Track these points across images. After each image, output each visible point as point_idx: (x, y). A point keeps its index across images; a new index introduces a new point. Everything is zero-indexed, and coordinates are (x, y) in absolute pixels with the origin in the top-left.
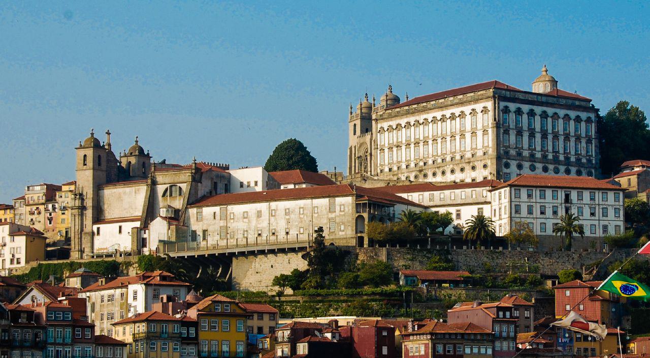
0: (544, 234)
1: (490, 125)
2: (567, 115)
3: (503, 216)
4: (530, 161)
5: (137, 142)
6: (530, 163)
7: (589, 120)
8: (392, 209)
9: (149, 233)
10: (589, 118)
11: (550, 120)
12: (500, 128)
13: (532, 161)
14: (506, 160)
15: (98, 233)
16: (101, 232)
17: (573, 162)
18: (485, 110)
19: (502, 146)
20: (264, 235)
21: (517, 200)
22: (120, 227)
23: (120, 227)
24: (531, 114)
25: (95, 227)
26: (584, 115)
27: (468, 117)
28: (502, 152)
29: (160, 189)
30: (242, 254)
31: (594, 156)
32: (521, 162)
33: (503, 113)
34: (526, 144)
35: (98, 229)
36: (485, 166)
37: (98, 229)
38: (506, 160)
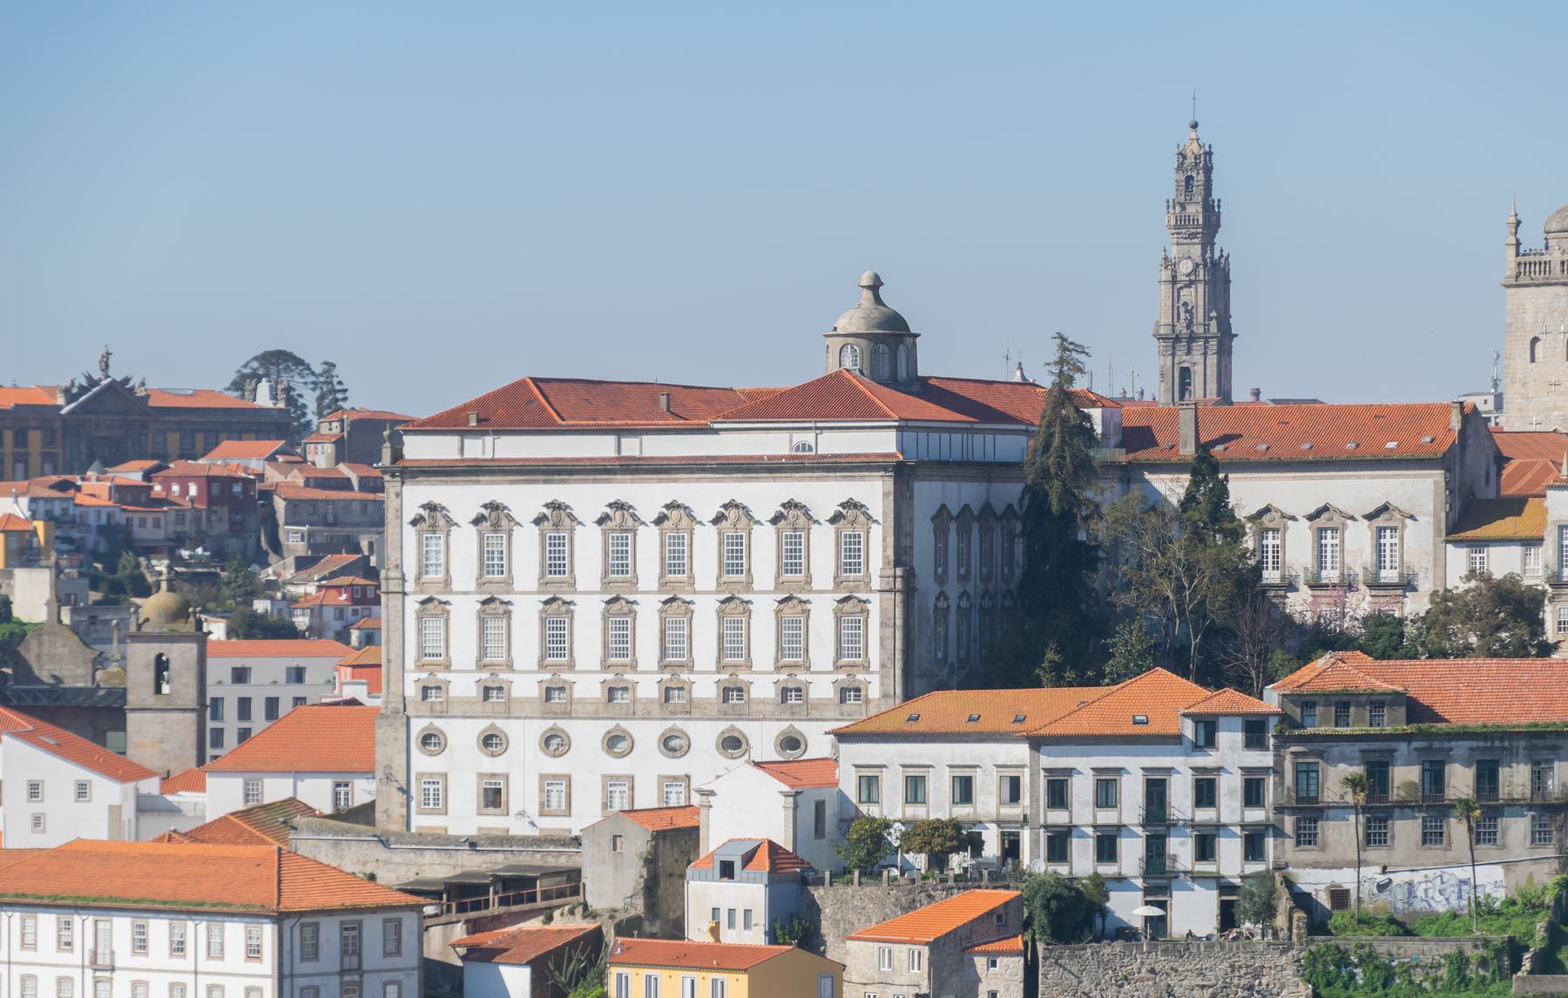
12: (404, 594)
13: (555, 715)
14: (424, 723)
17: (763, 702)
28: (412, 691)
31: (875, 665)
32: (499, 723)
38: (424, 723)
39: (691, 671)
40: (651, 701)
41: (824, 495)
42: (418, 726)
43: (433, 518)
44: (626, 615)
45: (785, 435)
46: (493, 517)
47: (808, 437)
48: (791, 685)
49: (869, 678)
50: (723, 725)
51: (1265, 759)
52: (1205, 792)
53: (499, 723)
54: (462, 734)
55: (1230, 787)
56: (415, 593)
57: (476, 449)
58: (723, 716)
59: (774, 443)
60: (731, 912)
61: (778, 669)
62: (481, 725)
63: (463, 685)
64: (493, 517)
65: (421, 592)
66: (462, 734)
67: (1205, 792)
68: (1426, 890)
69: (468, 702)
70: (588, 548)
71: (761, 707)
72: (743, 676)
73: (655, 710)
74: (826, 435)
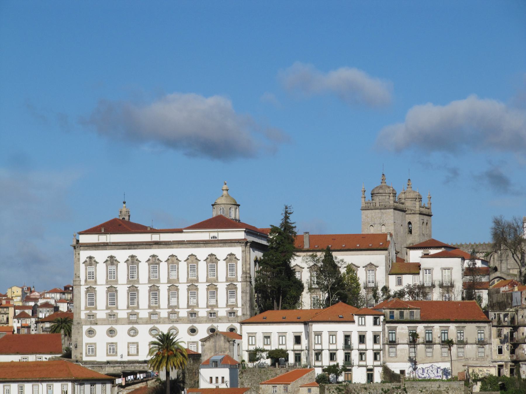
17: (203, 317)
19: (83, 307)
28: (83, 316)
31: (240, 305)
32: (114, 326)
33: (86, 266)
39: (179, 308)
40: (165, 318)
41: (222, 252)
42: (85, 328)
43: (91, 262)
44: (156, 291)
45: (208, 234)
46: (112, 261)
47: (215, 234)
48: (212, 312)
49: (237, 309)
50: (190, 325)
51: (379, 329)
52: (362, 339)
53: (114, 326)
54: (101, 330)
55: (369, 338)
56: (85, 285)
57: (103, 238)
58: (190, 322)
59: (204, 235)
60: (217, 378)
61: (207, 307)
62: (108, 327)
64: (112, 261)
65: (87, 285)
66: (101, 330)
67: (362, 339)
68: (427, 371)
69: (104, 320)
70: (144, 269)
71: (202, 319)
72: (196, 310)
73: (167, 320)
74: (220, 234)
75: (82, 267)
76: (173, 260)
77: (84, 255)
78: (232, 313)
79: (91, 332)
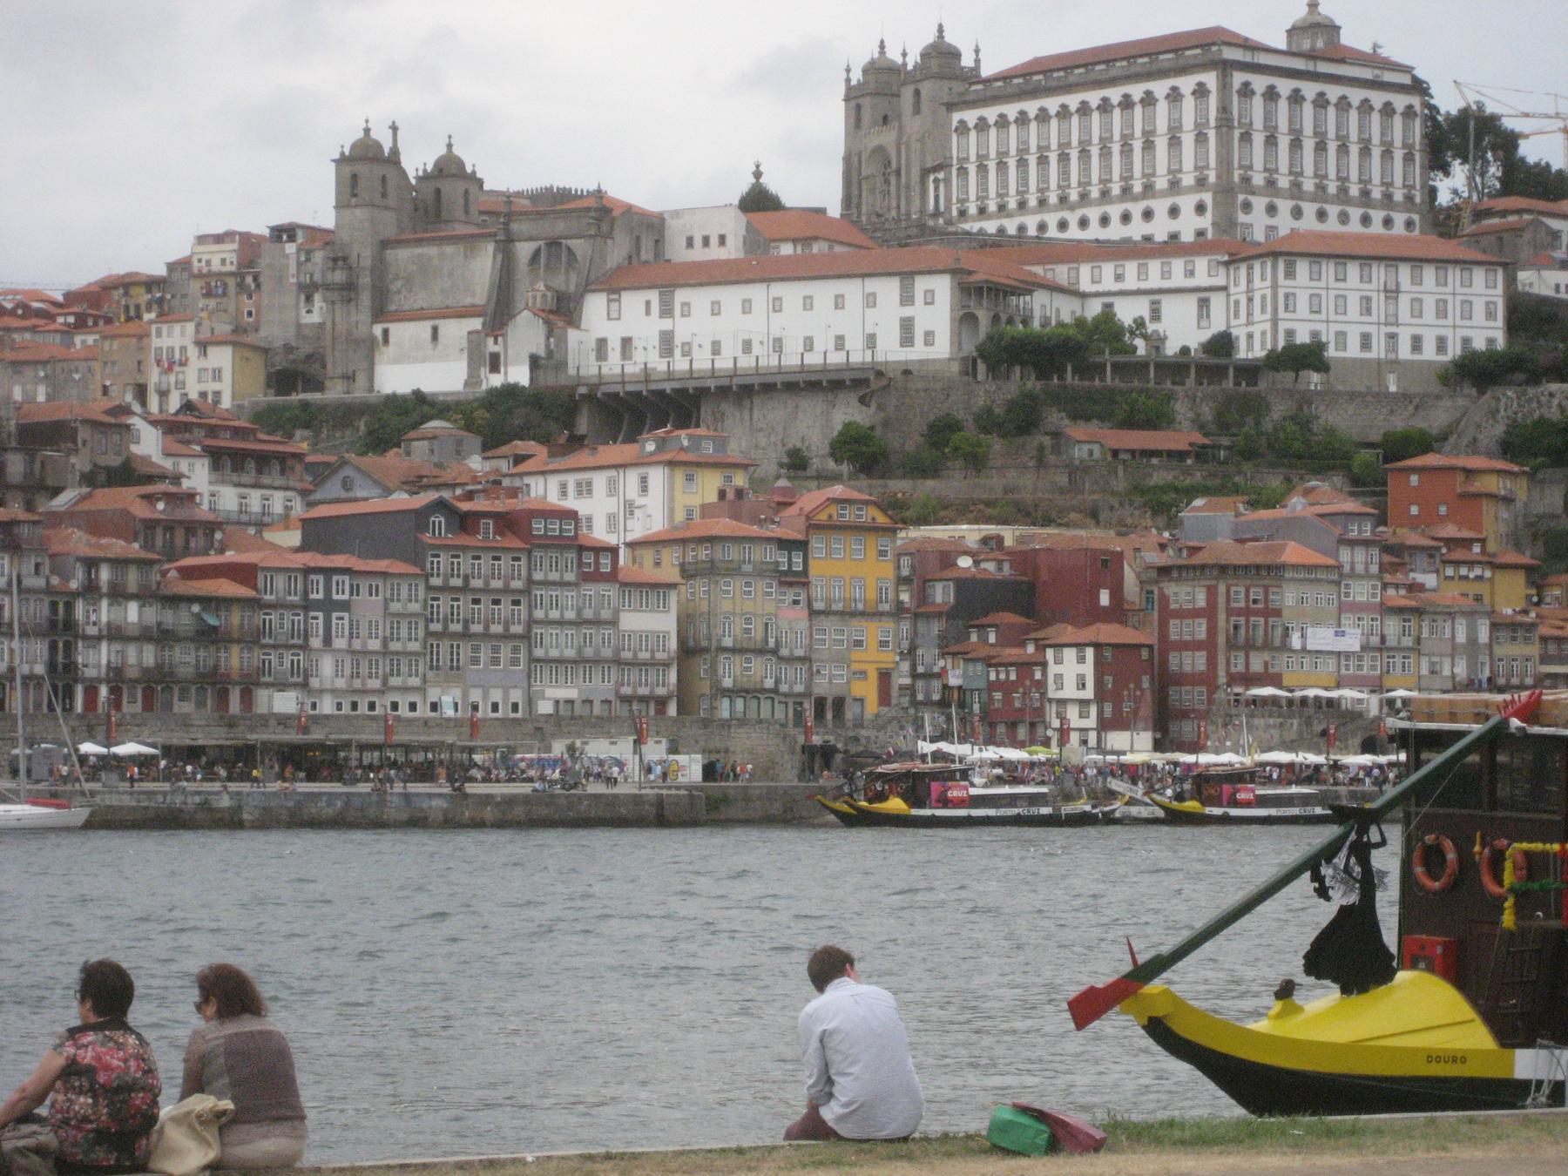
0: (1417, 357)
1: (1213, 123)
2: (1366, 101)
3: (1257, 315)
4: (1292, 198)
5: (450, 146)
6: (1292, 203)
7: (1409, 112)
8: (1028, 298)
9: (505, 342)
10: (1410, 107)
11: (1331, 111)
15: (386, 340)
16: (392, 339)
18: (1201, 92)
19: (1236, 164)
20: (757, 349)
21: (1290, 283)
22: (435, 330)
23: (435, 330)
24: (1296, 98)
25: (378, 330)
26: (1400, 101)
27: (1162, 108)
28: (1236, 179)
29: (524, 250)
30: (724, 391)
34: (1284, 165)
35: (386, 332)
36: (1200, 209)
37: (386, 332)
42: (1241, 197)
43: (1246, 91)
46: (1271, 94)
47: (1377, 72)
54: (1259, 203)
63: (1258, 179)
64: (1271, 94)
66: (1259, 203)
75: (1235, 98)
76: (1343, 105)
77: (1238, 78)
78: (1409, 198)
79: (1247, 207)
